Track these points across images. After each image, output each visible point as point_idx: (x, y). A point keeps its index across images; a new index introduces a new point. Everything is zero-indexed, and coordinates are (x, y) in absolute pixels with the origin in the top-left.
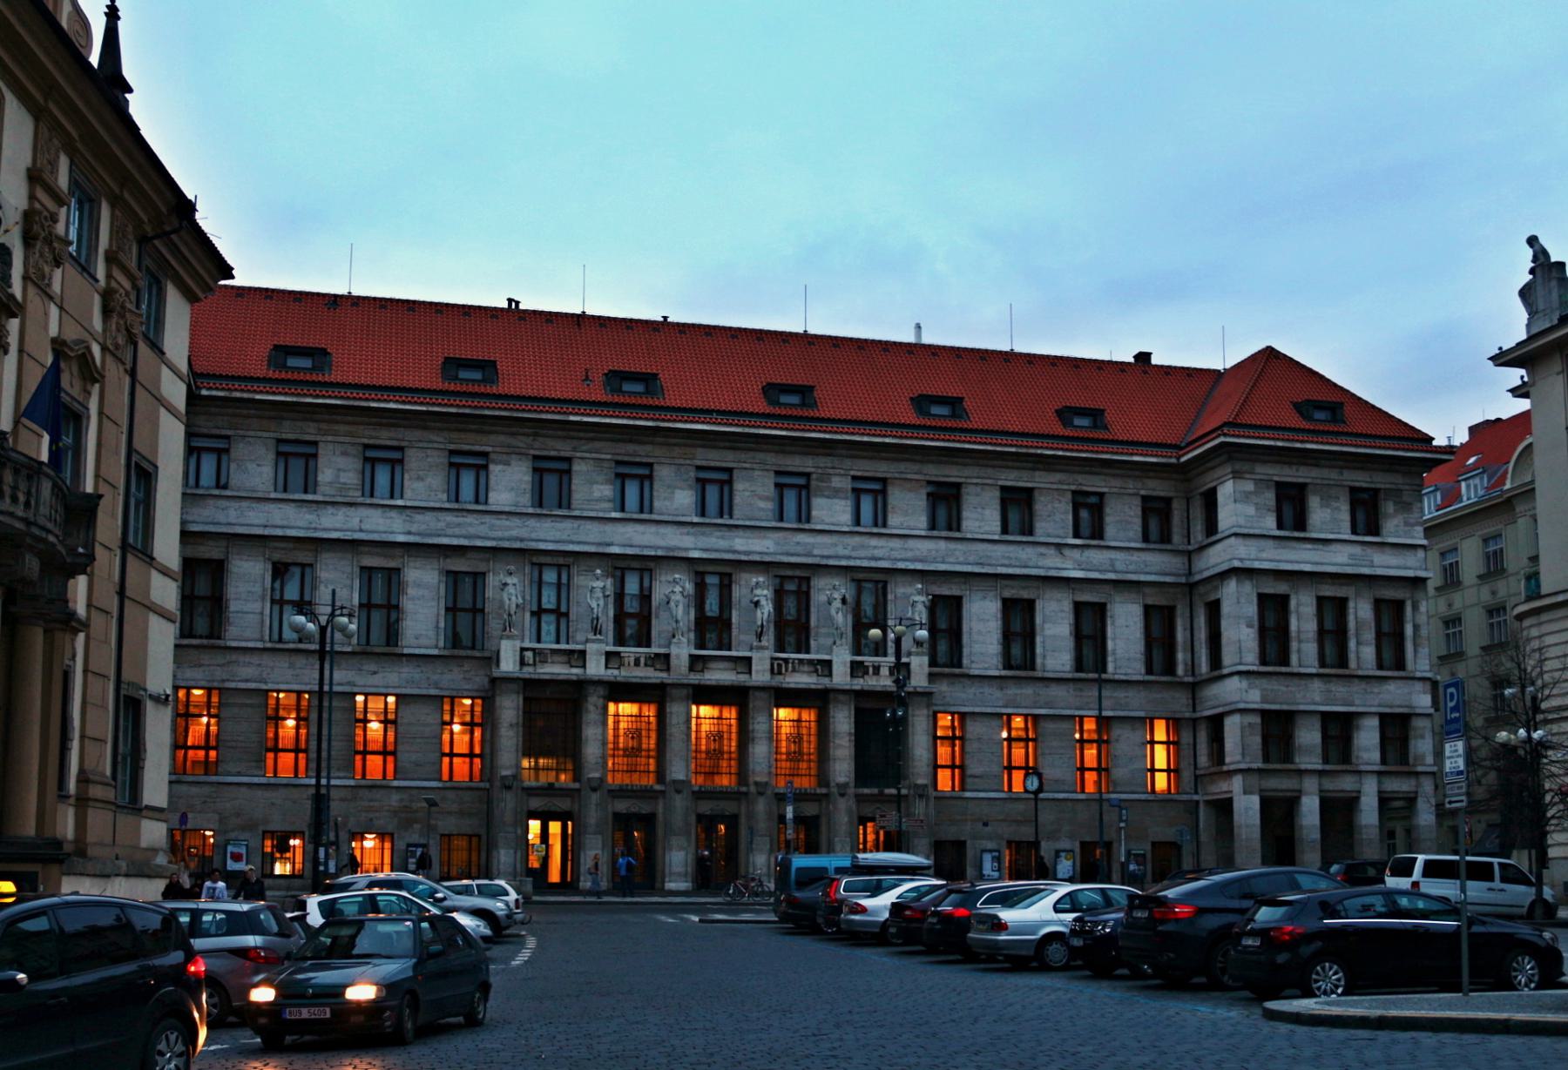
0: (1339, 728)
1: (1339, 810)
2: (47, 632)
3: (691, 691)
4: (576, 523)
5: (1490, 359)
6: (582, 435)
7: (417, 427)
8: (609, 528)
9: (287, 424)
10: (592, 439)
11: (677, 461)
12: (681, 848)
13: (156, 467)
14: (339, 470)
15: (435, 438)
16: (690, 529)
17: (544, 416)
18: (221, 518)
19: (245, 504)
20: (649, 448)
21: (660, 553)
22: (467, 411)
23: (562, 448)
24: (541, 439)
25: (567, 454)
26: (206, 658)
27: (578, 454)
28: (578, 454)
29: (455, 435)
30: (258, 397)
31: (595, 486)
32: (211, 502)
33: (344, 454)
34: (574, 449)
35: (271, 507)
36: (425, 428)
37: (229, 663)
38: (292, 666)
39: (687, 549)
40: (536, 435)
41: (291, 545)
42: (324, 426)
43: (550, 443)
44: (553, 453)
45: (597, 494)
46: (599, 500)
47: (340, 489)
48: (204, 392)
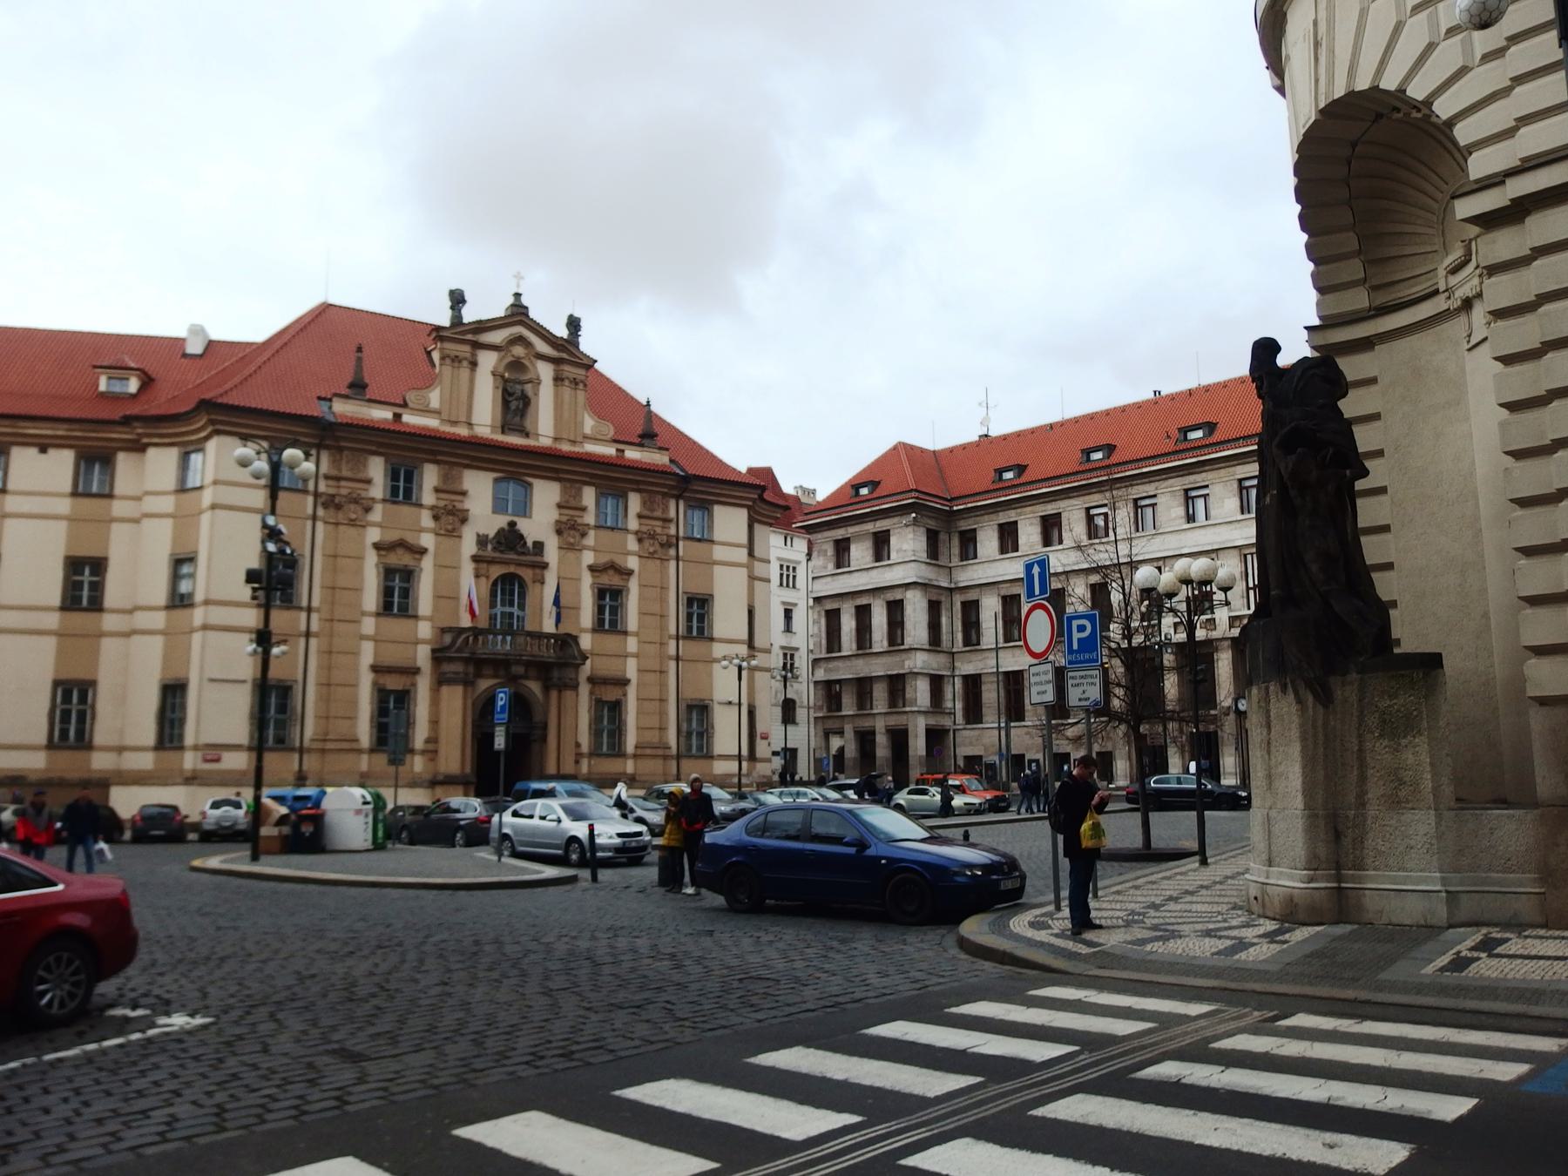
0: (897, 684)
1: (899, 738)
2: (560, 691)
3: (1230, 642)
4: (1163, 536)
5: (1306, 328)
6: (1158, 478)
7: (1065, 498)
8: (1183, 536)
9: (1001, 514)
10: (1166, 479)
11: (1224, 479)
12: (1231, 755)
13: (712, 596)
14: (1029, 535)
15: (1076, 503)
16: (1237, 525)
17: (1127, 473)
18: (975, 576)
19: (986, 565)
20: (1204, 475)
21: (1215, 547)
22: (1084, 482)
23: (1149, 489)
24: (1136, 487)
25: (1152, 493)
26: (973, 657)
27: (1159, 491)
28: (1159, 491)
29: (1087, 498)
30: (979, 504)
31: (1172, 510)
32: (970, 567)
33: (1031, 524)
34: (1157, 489)
35: (998, 564)
36: (1070, 498)
37: (984, 658)
38: (1014, 656)
39: (1233, 540)
40: (1132, 485)
41: (1008, 585)
42: (1019, 510)
43: (1141, 488)
44: (1145, 495)
45: (1174, 515)
46: (1175, 519)
47: (1031, 546)
48: (955, 508)
